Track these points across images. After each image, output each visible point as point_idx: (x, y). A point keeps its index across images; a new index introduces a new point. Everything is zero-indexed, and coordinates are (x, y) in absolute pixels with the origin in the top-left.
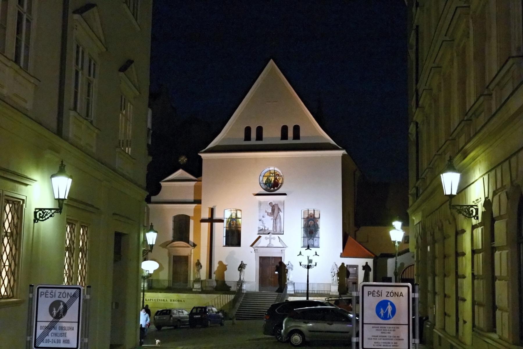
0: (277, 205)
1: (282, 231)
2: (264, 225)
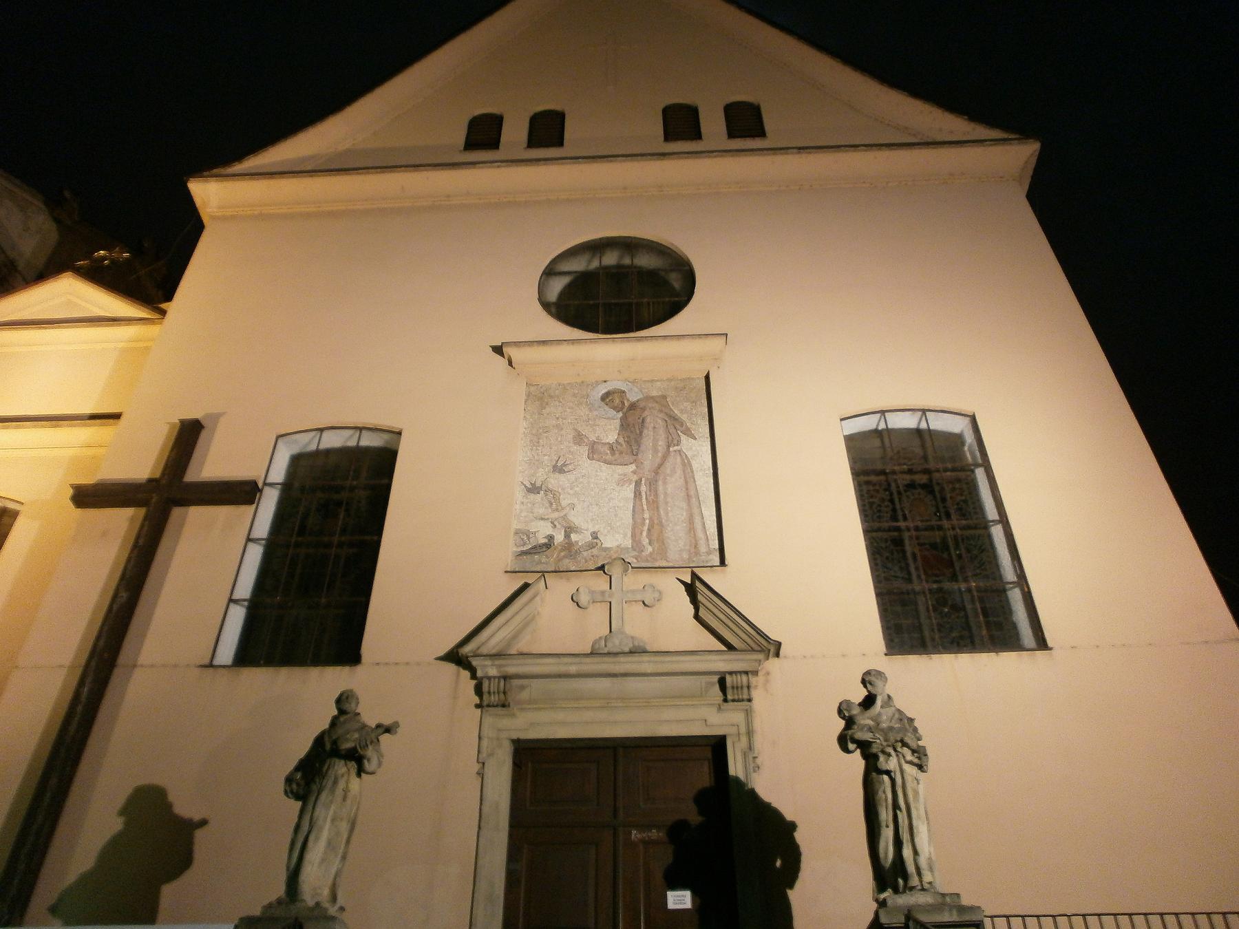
1: (709, 553)
2: (565, 517)
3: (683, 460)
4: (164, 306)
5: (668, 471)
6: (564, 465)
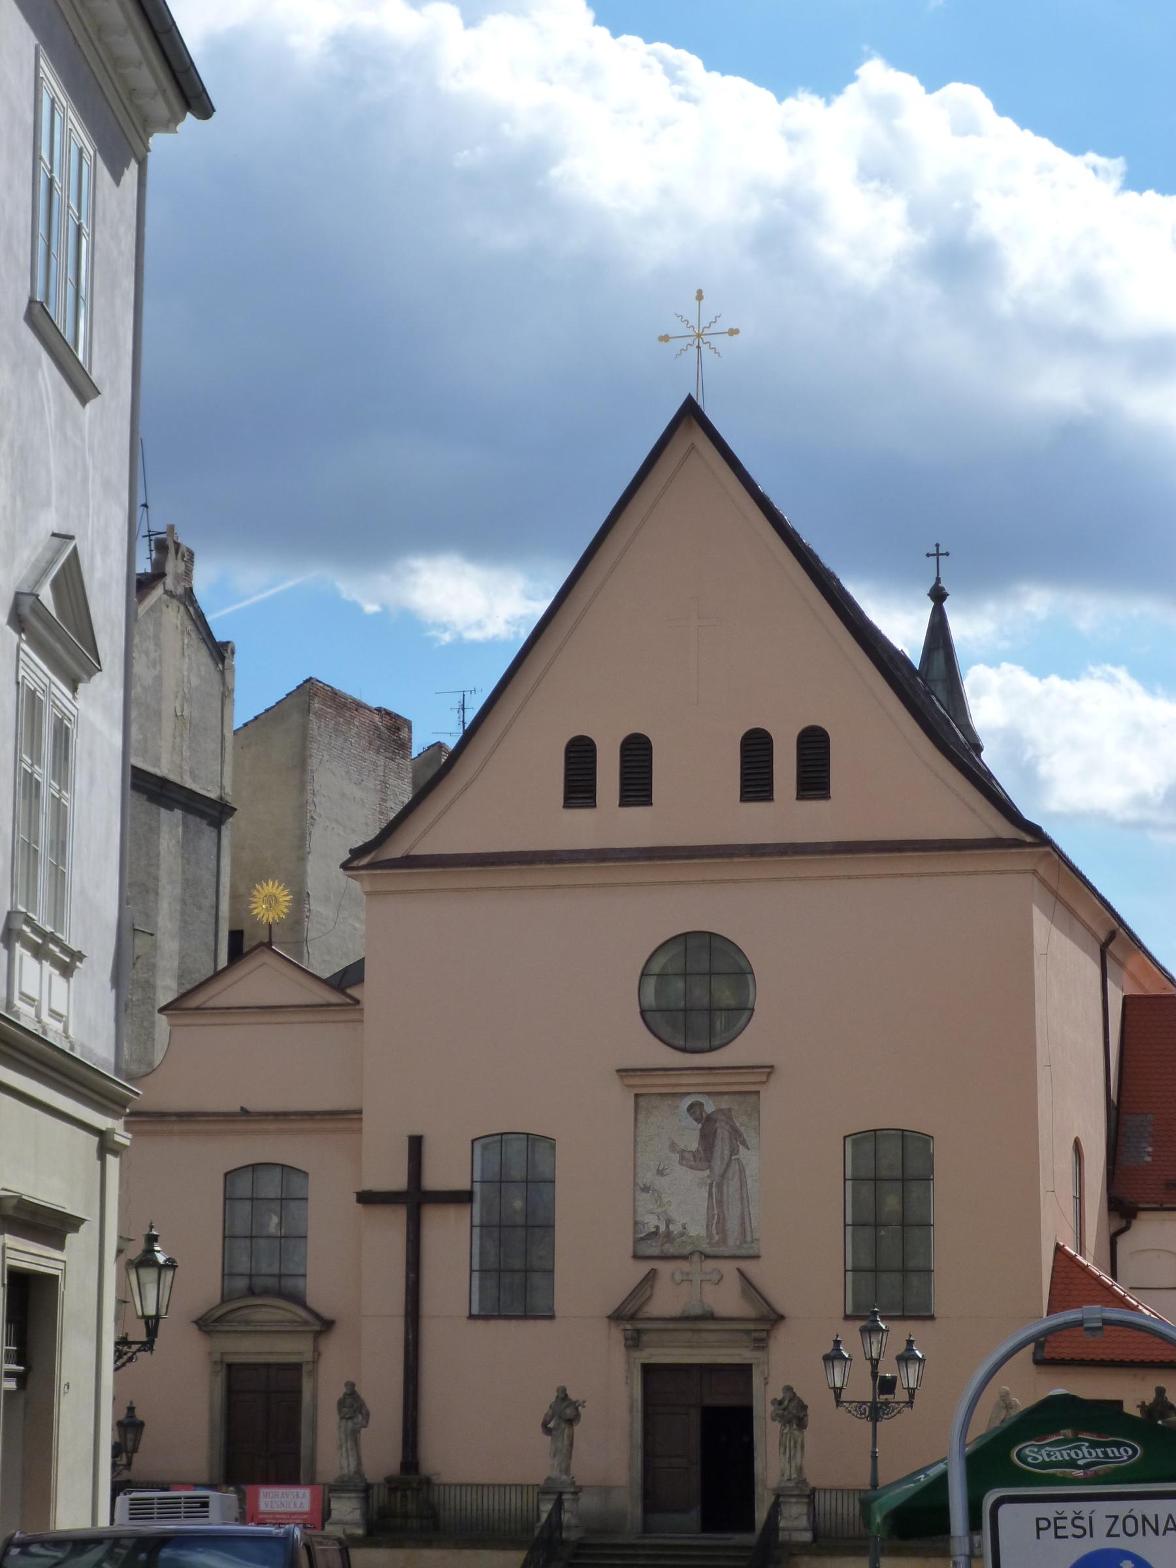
0: (727, 1114)
3: (740, 1169)
4: (353, 991)
5: (730, 1176)
6: (664, 1169)
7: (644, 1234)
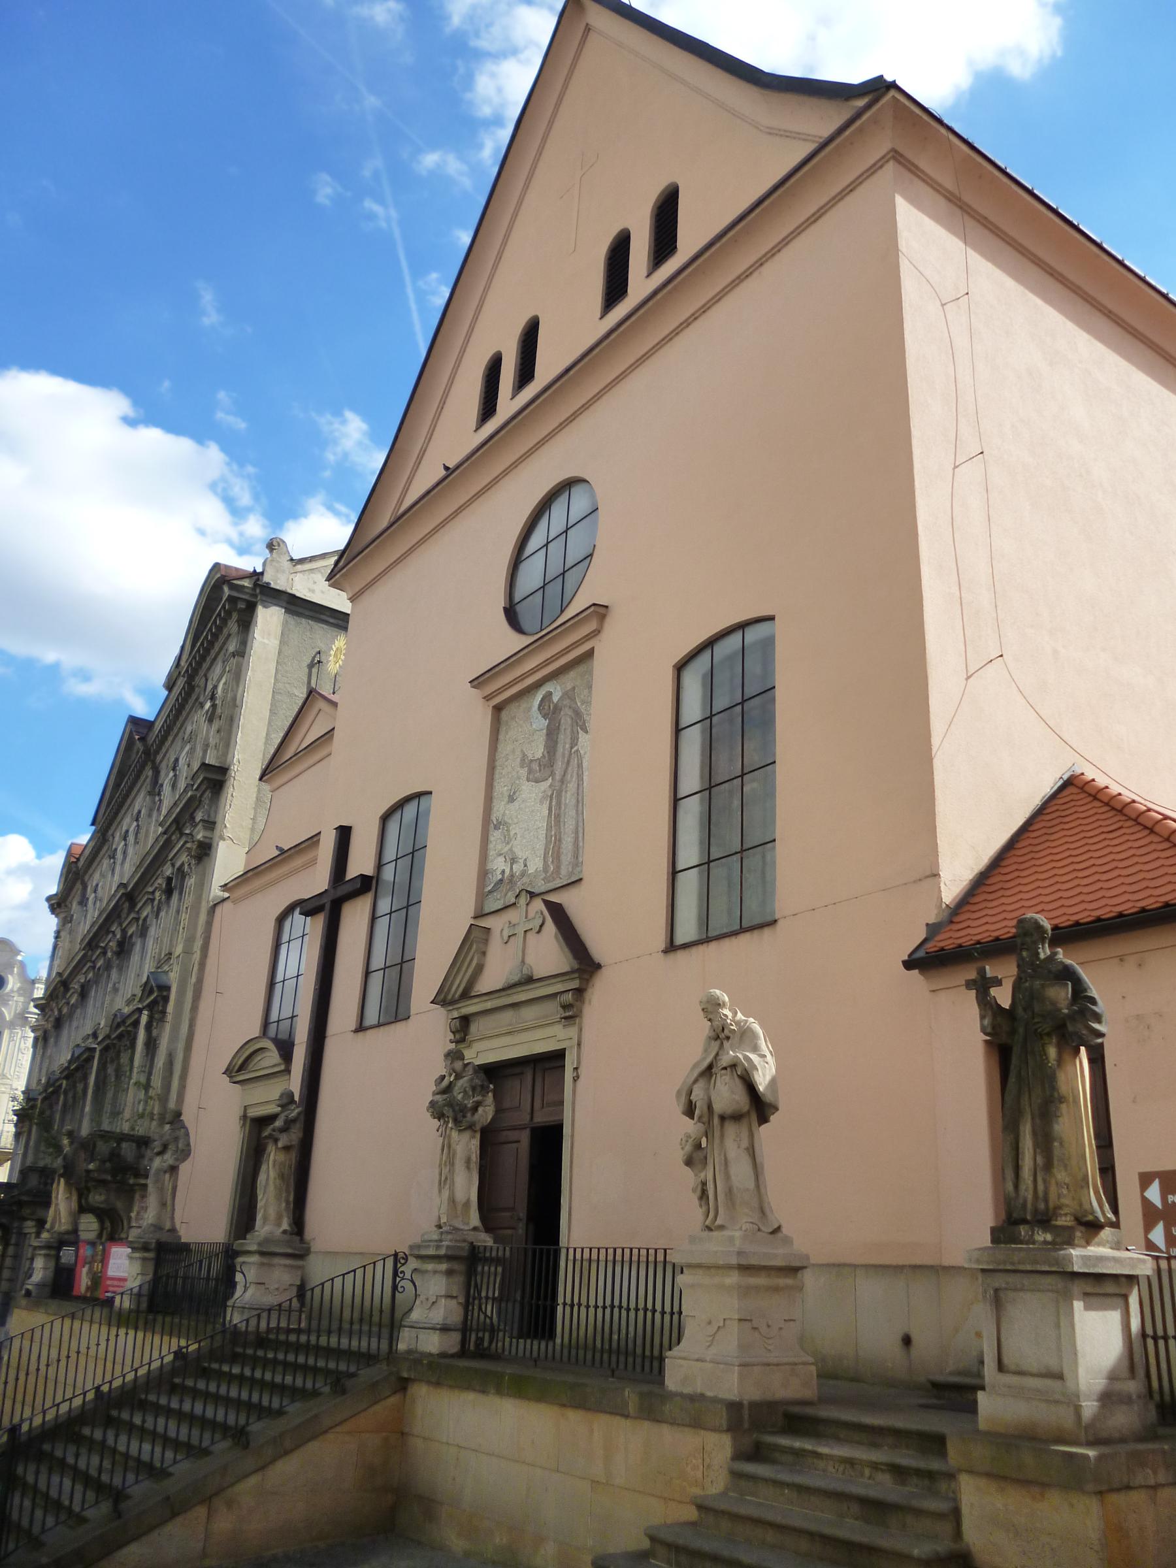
2: (511, 850)
3: (578, 760)
7: (492, 885)
